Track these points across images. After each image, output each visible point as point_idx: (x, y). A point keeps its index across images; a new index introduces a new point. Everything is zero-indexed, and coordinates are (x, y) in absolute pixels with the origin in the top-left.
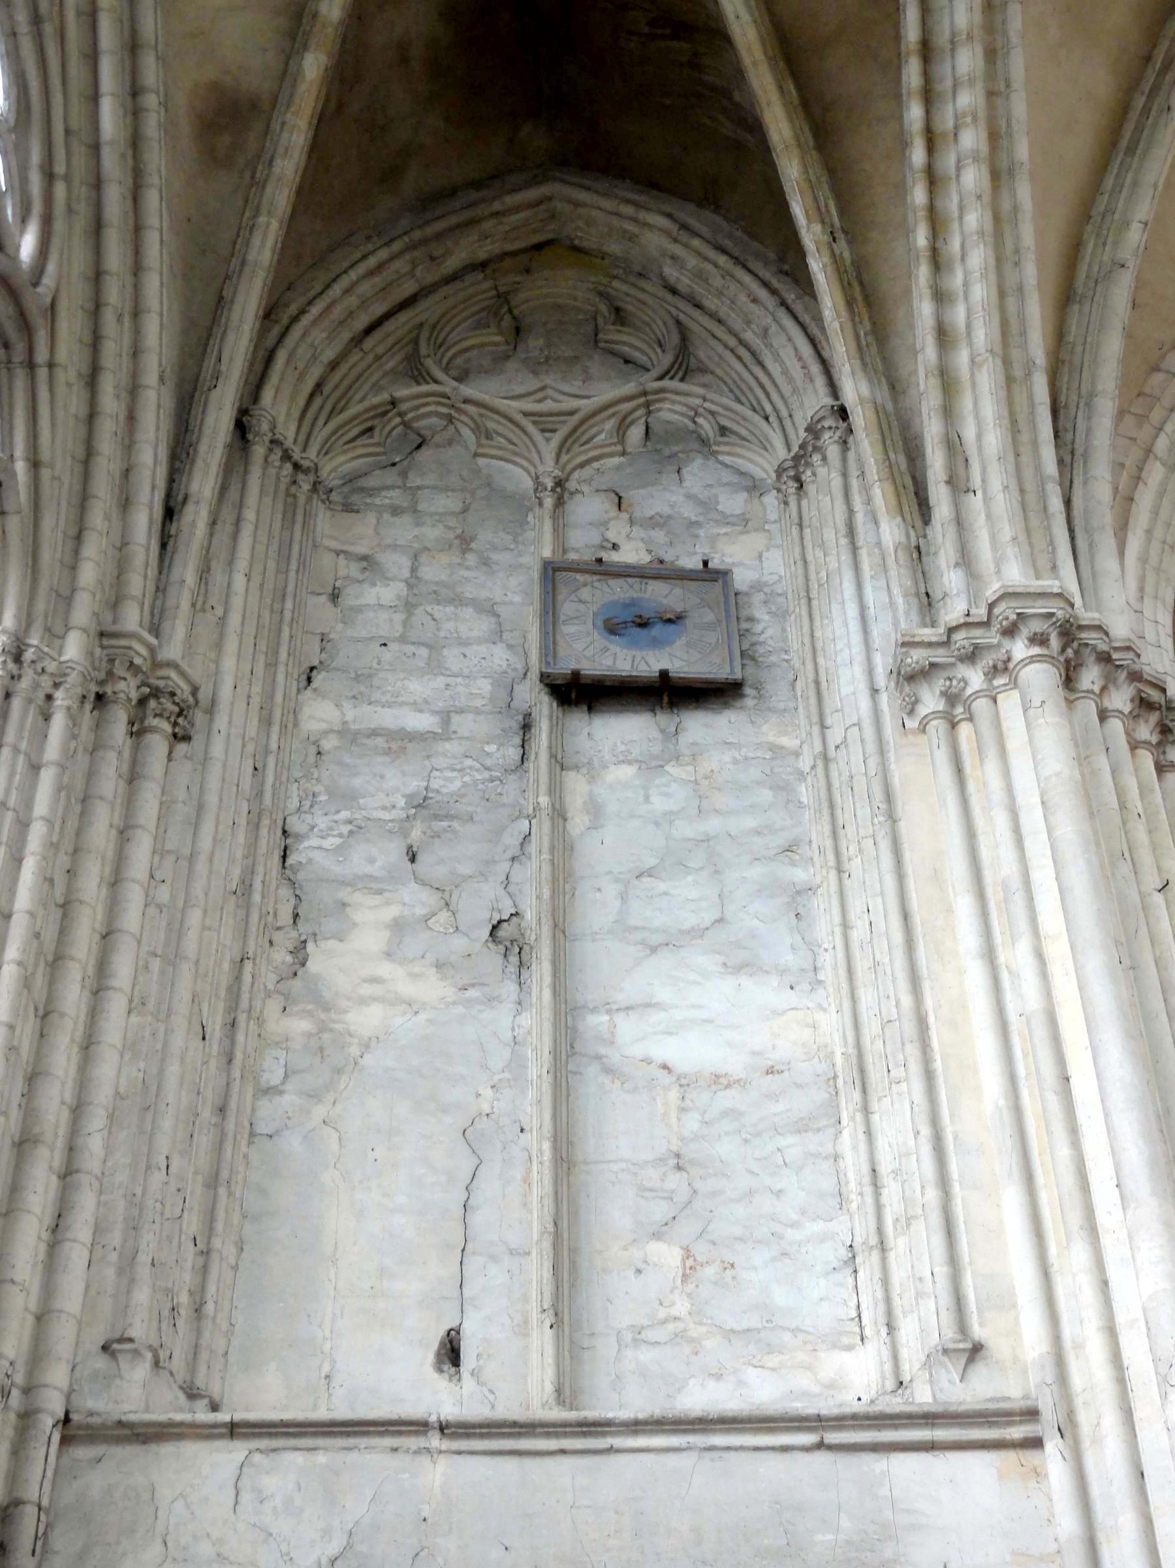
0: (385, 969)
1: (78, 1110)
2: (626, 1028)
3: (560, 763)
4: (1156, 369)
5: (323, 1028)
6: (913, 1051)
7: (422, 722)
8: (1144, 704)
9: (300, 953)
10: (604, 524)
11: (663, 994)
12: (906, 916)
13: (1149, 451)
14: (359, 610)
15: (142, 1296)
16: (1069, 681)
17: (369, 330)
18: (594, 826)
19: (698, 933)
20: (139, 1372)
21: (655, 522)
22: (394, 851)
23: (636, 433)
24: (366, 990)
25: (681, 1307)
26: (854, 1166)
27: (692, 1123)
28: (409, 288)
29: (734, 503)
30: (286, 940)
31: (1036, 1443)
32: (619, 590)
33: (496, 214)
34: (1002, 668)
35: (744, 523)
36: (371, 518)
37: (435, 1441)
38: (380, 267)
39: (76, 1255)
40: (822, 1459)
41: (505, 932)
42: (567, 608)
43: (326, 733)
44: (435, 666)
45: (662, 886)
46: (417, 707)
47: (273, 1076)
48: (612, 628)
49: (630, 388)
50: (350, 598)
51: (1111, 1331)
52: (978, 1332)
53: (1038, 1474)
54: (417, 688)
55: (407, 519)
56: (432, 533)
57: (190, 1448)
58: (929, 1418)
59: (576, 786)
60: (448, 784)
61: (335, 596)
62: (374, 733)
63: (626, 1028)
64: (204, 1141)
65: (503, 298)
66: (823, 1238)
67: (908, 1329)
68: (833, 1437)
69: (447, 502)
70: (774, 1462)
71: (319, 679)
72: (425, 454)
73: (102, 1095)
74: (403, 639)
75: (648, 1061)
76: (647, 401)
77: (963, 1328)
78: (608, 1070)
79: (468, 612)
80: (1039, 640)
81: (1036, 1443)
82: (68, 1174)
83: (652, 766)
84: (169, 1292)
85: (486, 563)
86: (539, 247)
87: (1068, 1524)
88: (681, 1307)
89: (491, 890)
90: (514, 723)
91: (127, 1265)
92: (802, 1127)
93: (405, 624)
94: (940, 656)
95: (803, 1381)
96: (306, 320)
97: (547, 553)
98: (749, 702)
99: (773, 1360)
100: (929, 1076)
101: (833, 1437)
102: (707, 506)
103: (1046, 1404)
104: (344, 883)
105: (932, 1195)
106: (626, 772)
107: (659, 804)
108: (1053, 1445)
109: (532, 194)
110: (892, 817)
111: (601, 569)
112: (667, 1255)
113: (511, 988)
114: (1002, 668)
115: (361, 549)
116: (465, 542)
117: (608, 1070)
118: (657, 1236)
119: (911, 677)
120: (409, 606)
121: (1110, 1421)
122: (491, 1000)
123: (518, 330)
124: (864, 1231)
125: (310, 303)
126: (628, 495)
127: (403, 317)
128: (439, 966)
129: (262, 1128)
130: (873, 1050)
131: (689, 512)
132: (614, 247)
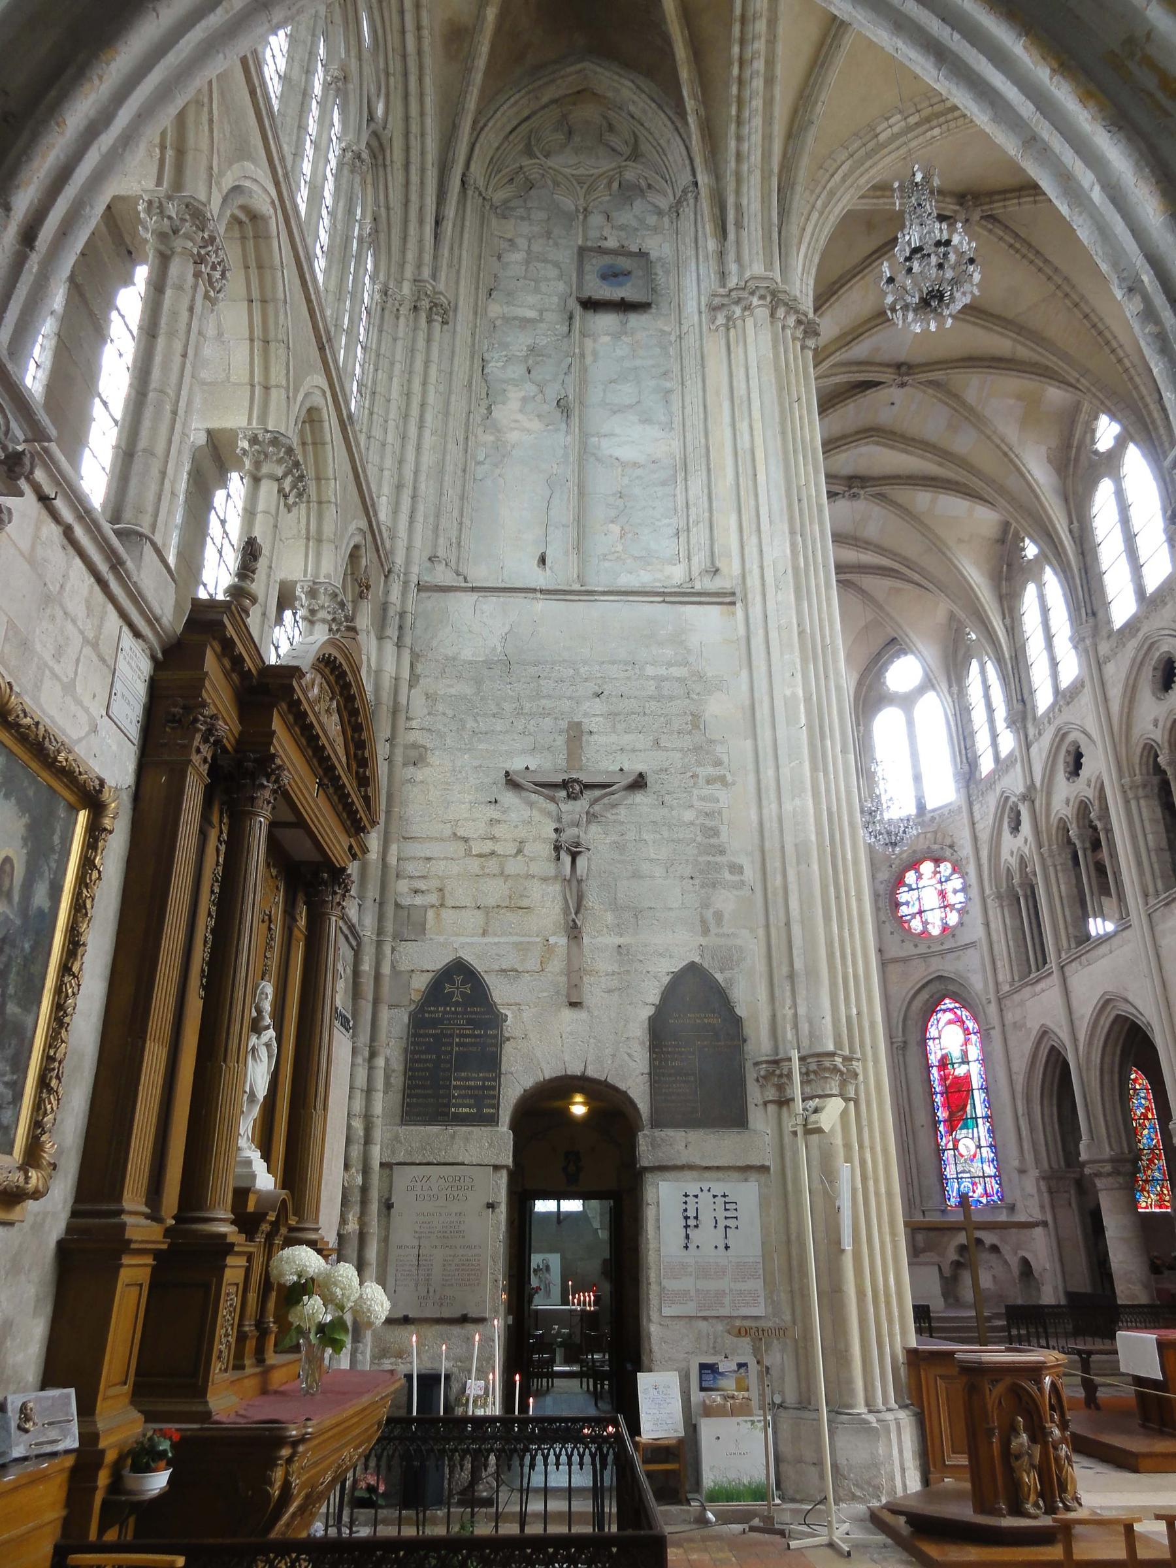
0: (520, 417)
1: (416, 473)
2: (605, 443)
4: (821, 167)
5: (498, 439)
6: (704, 460)
7: (532, 314)
8: (799, 322)
9: (489, 408)
10: (602, 228)
11: (617, 431)
12: (705, 407)
13: (813, 206)
14: (508, 264)
15: (441, 541)
16: (772, 315)
17: (511, 132)
18: (595, 361)
19: (631, 406)
20: (440, 568)
21: (622, 228)
22: (522, 370)
23: (615, 185)
24: (513, 425)
25: (620, 548)
26: (680, 499)
27: (626, 481)
28: (526, 113)
29: (652, 220)
30: (484, 403)
31: (733, 603)
32: (607, 260)
33: (562, 77)
34: (747, 308)
35: (656, 230)
36: (513, 221)
37: (539, 595)
38: (516, 103)
39: (419, 527)
40: (664, 605)
41: (562, 403)
42: (588, 268)
43: (497, 318)
44: (537, 290)
45: (619, 387)
46: (531, 307)
47: (481, 457)
48: (604, 277)
49: (613, 165)
50: (504, 260)
51: (762, 568)
52: (718, 564)
53: (734, 614)
54: (531, 299)
55: (526, 223)
56: (536, 229)
57: (459, 594)
58: (699, 594)
59: (589, 343)
60: (543, 341)
61: (499, 257)
62: (515, 318)
63: (605, 443)
64: (459, 483)
65: (565, 116)
66: (669, 525)
67: (695, 560)
68: (667, 599)
69: (542, 215)
70: (648, 606)
71: (494, 293)
72: (533, 192)
73: (424, 468)
74: (525, 278)
75: (611, 456)
76: (620, 169)
77: (713, 563)
78: (598, 459)
79: (549, 266)
80: (762, 297)
81: (733, 603)
82: (414, 497)
83: (616, 336)
84: (450, 539)
85: (556, 244)
86: (579, 92)
87: (742, 631)
88: (620, 548)
89: (557, 386)
90: (566, 316)
91: (436, 529)
92: (664, 484)
93: (526, 270)
94: (725, 301)
95: (659, 576)
96: (487, 129)
97: (580, 242)
98: (653, 311)
99: (649, 568)
100: (709, 470)
101: (667, 599)
102: (641, 221)
103: (738, 591)
104: (504, 382)
105: (707, 514)
106: (607, 339)
107: (619, 353)
108: (739, 605)
109: (579, 67)
110: (703, 367)
111: (601, 251)
112: (615, 529)
113: (564, 426)
114: (747, 308)
115: (509, 236)
117: (598, 459)
118: (612, 522)
119: (714, 309)
120: (527, 262)
121: (758, 598)
122: (557, 430)
123: (570, 133)
124: (682, 524)
125: (488, 120)
126: (614, 214)
127: (524, 126)
128: (539, 416)
129: (479, 477)
130: (690, 457)
131: (634, 224)
132: (610, 94)
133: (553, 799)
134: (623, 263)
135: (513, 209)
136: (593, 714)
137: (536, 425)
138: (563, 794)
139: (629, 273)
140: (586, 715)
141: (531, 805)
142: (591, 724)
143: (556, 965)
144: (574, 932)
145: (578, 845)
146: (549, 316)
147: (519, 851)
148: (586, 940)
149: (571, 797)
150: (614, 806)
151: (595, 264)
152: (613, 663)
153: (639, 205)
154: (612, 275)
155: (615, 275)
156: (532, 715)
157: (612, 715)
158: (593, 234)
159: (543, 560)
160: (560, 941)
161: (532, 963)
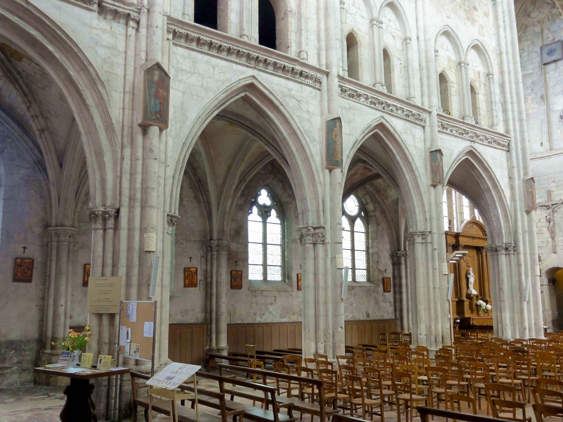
3: (545, 73)
7: (531, 71)
10: (547, 34)
18: (549, 81)
21: (553, 32)
23: (550, 17)
32: (549, 47)
48: (548, 54)
54: (530, 67)
56: (529, 42)
59: (548, 76)
60: (535, 79)
62: (526, 75)
78: (553, 112)
83: (555, 70)
106: (552, 72)
111: (547, 45)
112: (559, 131)
116: (533, 43)
117: (553, 112)
120: (528, 55)
122: (542, 105)
123: (535, 3)
133: (544, 209)
134: (554, 46)
135: (522, 38)
136: (553, 187)
137: (536, 106)
138: (546, 208)
139: (555, 50)
140: (551, 187)
141: (541, 211)
142: (553, 189)
143: (550, 245)
144: (553, 238)
145: (550, 220)
146: (536, 70)
147: (540, 221)
148: (556, 239)
149: (548, 209)
150: (559, 208)
151: (546, 50)
152: (557, 173)
153: (557, 21)
154: (550, 53)
155: (552, 52)
156: (539, 189)
157: (557, 186)
158: (545, 37)
159: (542, 143)
160: (550, 240)
161: (545, 245)
